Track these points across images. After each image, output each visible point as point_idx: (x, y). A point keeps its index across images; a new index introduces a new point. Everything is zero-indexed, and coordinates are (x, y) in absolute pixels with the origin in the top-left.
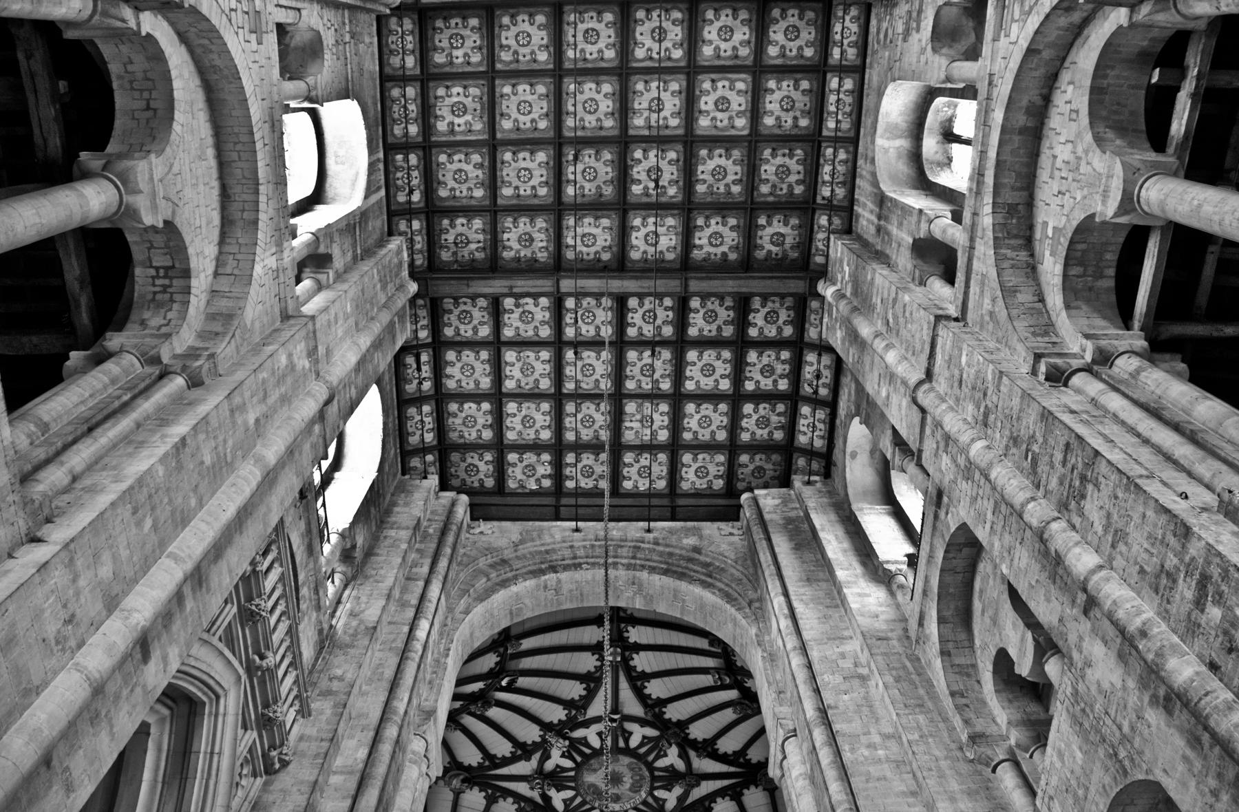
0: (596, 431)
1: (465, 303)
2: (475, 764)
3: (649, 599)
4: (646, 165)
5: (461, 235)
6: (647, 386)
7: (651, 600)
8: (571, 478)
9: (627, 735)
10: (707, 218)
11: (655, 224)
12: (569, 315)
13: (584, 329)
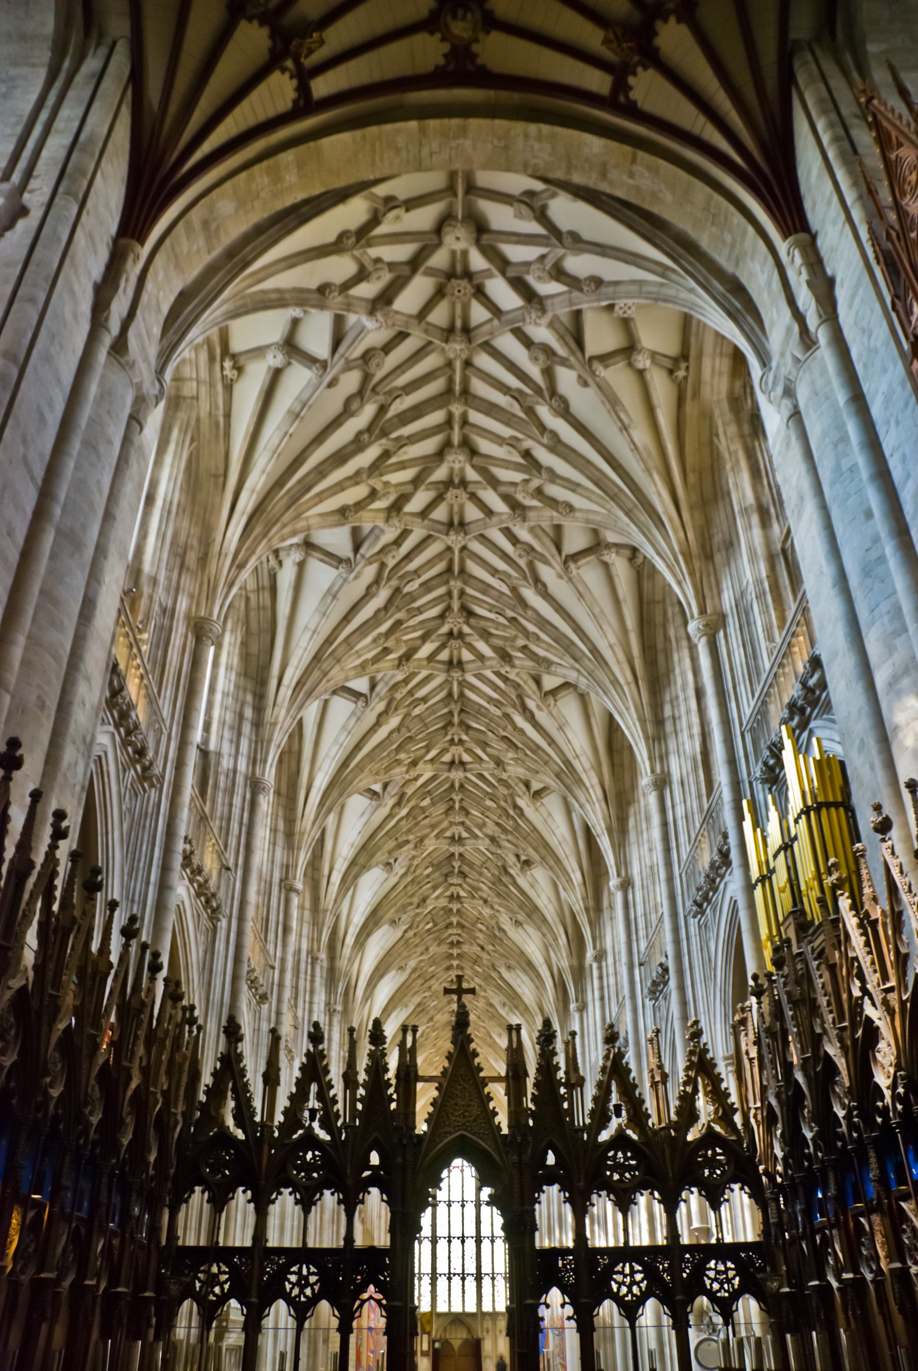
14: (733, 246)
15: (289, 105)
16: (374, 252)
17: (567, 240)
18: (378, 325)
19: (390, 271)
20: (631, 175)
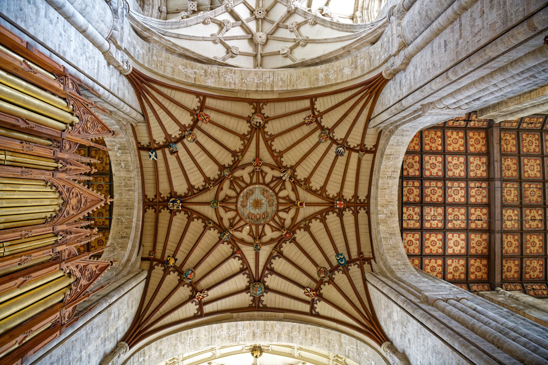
2: (266, 130)
3: (385, 222)
4: (536, 215)
6: (450, 217)
7: (384, 222)
9: (286, 211)
11: (515, 220)
13: (474, 191)
14: (152, 56)
15: (318, 99)
16: (293, 36)
18: (294, 3)
19: (287, 26)
20: (195, 73)
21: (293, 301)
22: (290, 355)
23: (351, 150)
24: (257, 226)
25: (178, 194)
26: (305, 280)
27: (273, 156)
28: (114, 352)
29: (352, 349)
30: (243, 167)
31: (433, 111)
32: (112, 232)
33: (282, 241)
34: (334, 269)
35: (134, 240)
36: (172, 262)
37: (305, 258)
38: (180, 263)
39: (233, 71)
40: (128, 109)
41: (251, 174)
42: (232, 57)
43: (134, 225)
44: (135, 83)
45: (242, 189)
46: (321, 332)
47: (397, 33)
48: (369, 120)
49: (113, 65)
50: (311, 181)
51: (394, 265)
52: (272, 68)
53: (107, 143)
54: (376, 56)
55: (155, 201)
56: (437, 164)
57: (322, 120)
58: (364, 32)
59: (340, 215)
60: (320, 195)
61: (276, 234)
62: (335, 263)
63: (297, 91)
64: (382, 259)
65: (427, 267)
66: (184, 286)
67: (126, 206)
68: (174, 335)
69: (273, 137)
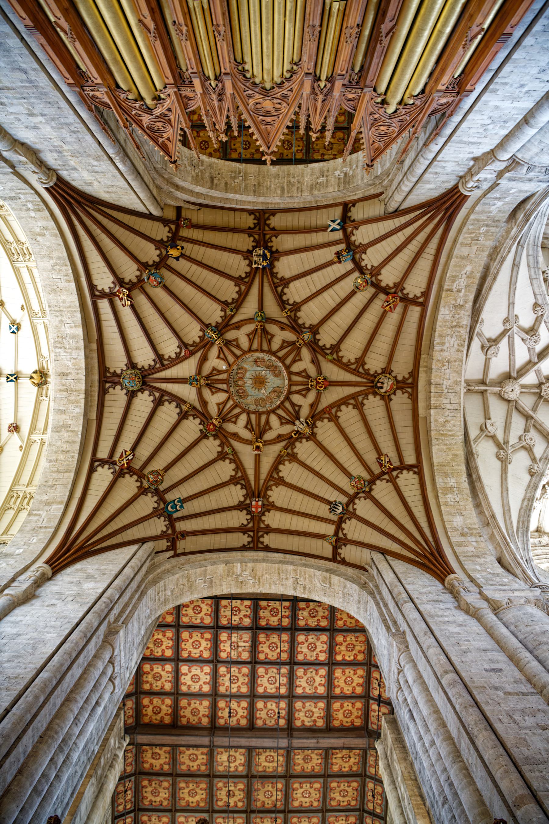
0: (268, 640)
1: (347, 722)
2: (371, 397)
3: (230, 573)
4: (235, 799)
5: (346, 762)
6: (234, 670)
7: (229, 572)
8: (285, 607)
9: (248, 426)
10: (199, 770)
11: (229, 767)
12: (283, 715)
13: (274, 706)
14: (487, 225)
15: (416, 476)
16: (513, 440)
17: (508, 325)
19: (528, 432)
20: (459, 291)
21: (114, 433)
22: (33, 428)
23: (339, 525)
24: (226, 381)
25: (276, 263)
26: (144, 451)
27: (331, 406)
28: (41, 164)
29: (41, 520)
30: (315, 362)
31: (395, 649)
32: (221, 162)
33: (203, 419)
34: (160, 495)
35: (208, 196)
36: (174, 253)
37: (178, 452)
38: (172, 266)
39: (461, 348)
40: (406, 188)
41: (303, 373)
42: (483, 347)
43: (231, 196)
44: (445, 199)
45: (282, 360)
46: (66, 475)
47: (515, 597)
48: (384, 552)
49: (473, 166)
50: (293, 463)
51: (165, 585)
52: (464, 407)
53: (354, 156)
54: (480, 564)
55: (267, 228)
56: (315, 653)
57: (384, 481)
58: (518, 548)
59: (241, 507)
60: (271, 476)
61: (213, 410)
62: (169, 497)
63: (429, 445)
64: (174, 567)
65: (161, 634)
66: (138, 270)
67: (259, 183)
68: (65, 255)
69: (359, 407)
